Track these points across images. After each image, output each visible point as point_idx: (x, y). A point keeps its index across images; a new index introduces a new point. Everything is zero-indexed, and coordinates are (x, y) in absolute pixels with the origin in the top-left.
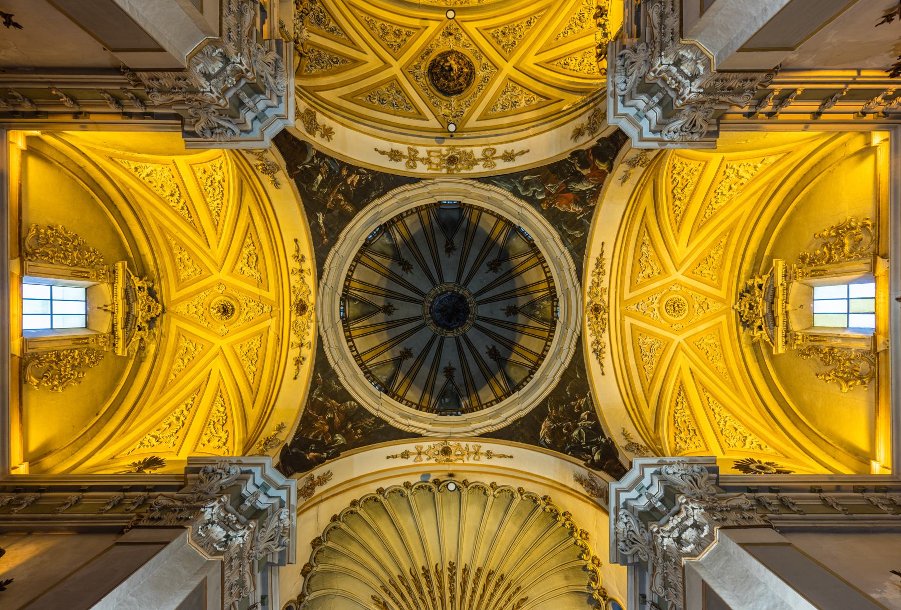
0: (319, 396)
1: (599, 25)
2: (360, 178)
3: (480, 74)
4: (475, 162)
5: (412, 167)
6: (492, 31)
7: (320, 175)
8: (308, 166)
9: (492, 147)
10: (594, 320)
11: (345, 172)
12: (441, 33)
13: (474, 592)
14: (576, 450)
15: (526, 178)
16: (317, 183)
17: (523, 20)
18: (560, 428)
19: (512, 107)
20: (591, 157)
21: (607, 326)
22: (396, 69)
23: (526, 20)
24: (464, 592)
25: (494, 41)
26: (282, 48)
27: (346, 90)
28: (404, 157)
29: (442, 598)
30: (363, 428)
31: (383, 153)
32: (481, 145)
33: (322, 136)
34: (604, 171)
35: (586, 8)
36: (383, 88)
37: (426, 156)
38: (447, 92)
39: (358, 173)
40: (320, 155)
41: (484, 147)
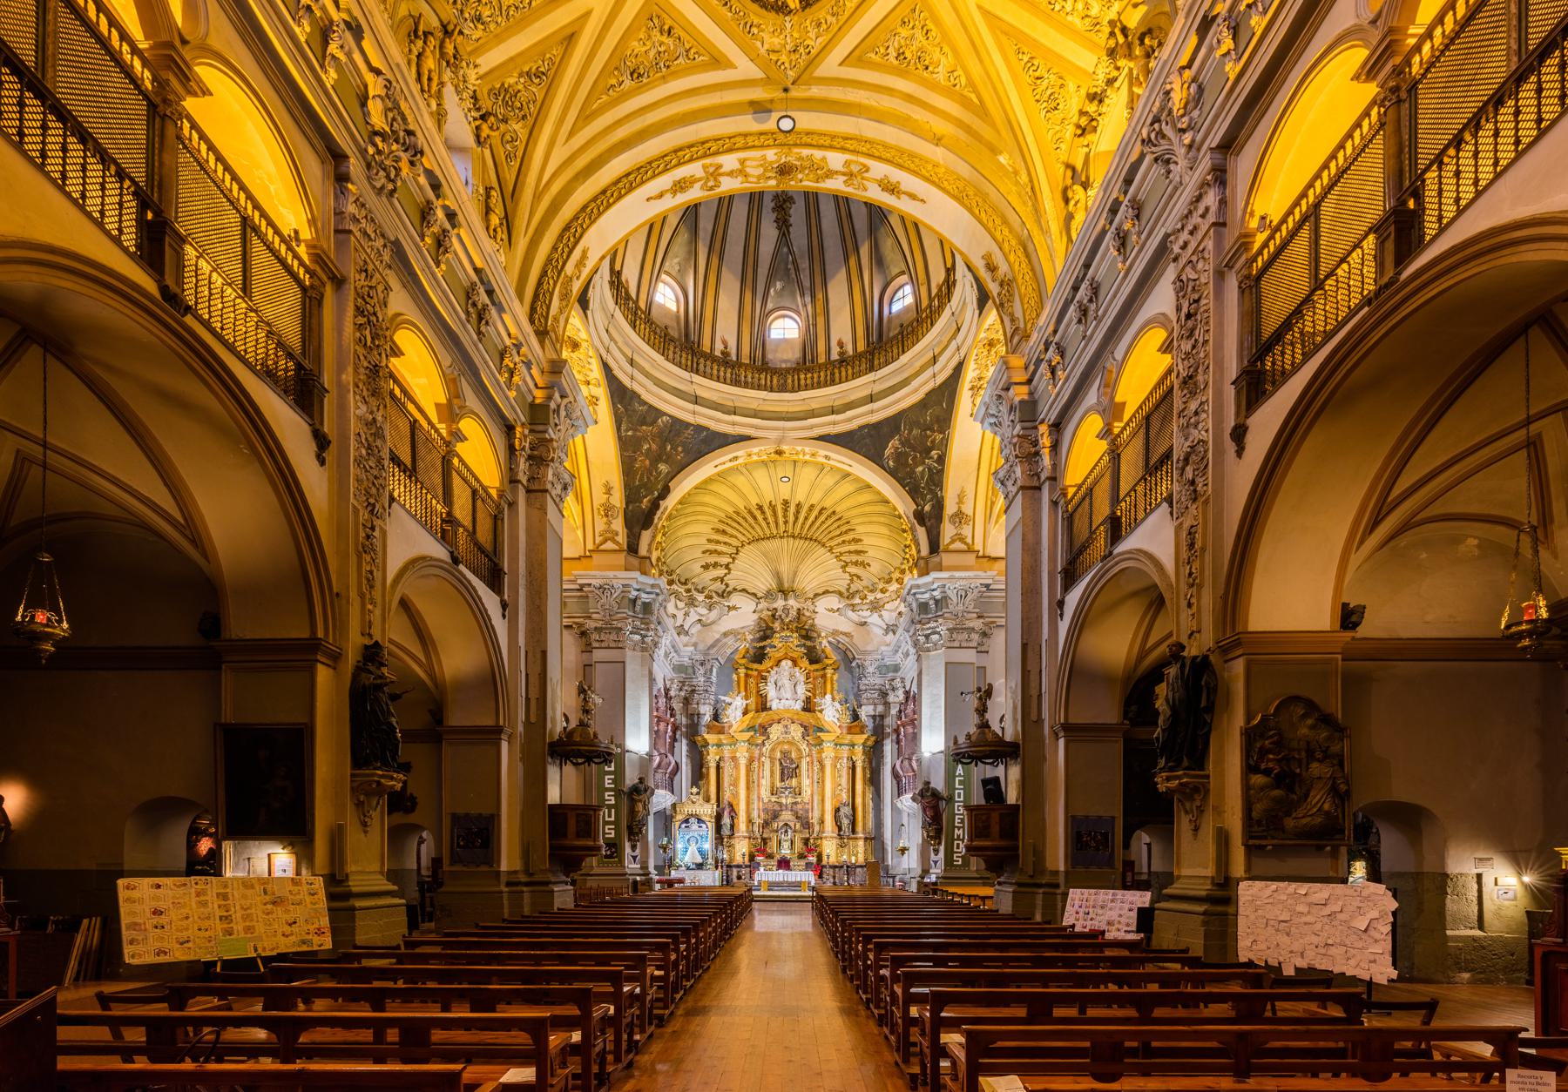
0: (627, 430)
4: (830, 174)
5: (711, 189)
13: (806, 518)
14: (914, 492)
18: (906, 455)
24: (796, 518)
29: (777, 523)
30: (683, 444)
37: (737, 166)
41: (848, 156)
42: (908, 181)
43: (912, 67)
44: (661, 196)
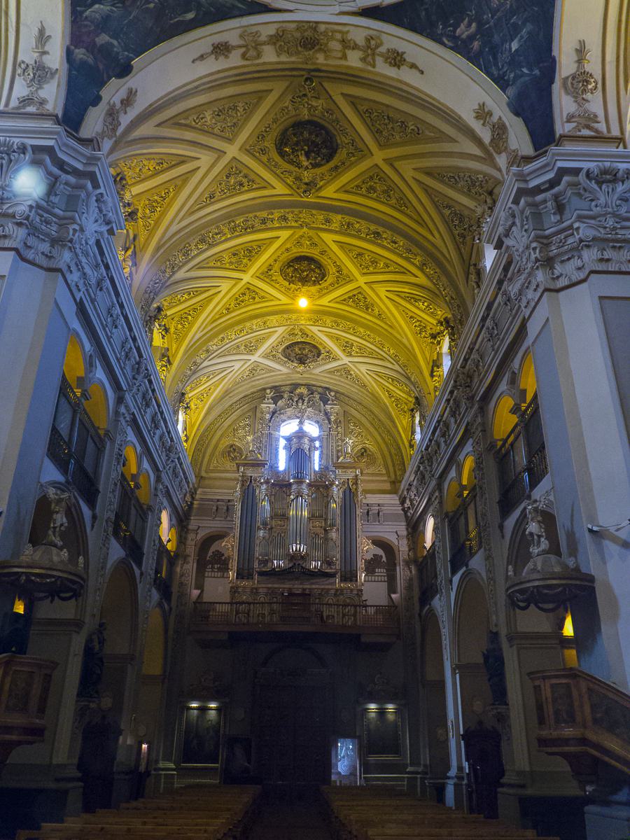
1: (129, 205)
2: (454, 31)
3: (269, 144)
6: (255, 186)
7: (513, 50)
8: (525, 70)
11: (476, 45)
15: (190, 16)
16: (522, 37)
17: (220, 198)
19: (224, 109)
20: (101, 67)
22: (379, 156)
23: (215, 199)
25: (252, 176)
27: (448, 147)
28: (381, 55)
31: (413, 66)
32: (264, 63)
33: (490, 114)
34: (76, 47)
35: (149, 218)
37: (350, 53)
38: (314, 125)
39: (454, 38)
40: (502, 83)
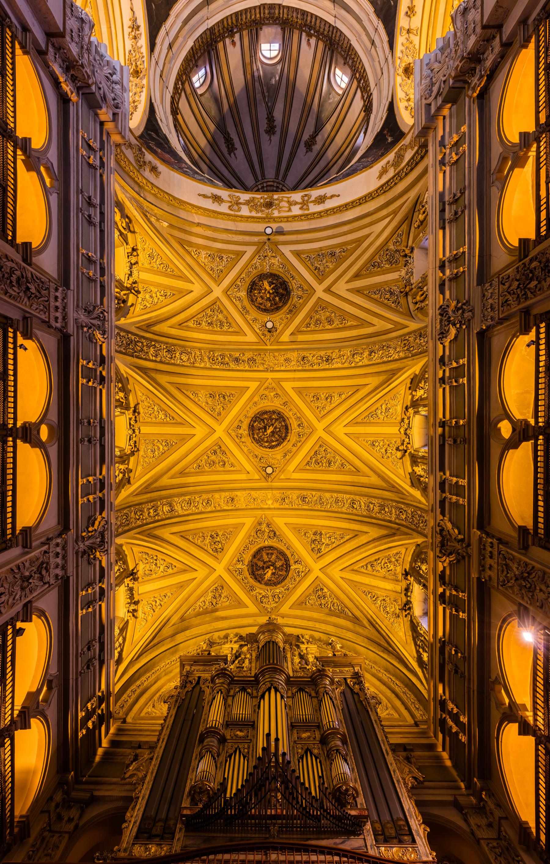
4: (247, 203)
5: (306, 195)
9: (232, 213)
10: (138, 63)
12: (278, 331)
21: (127, 58)
26: (425, 114)
36: (331, 266)
37: (293, 208)
42: (208, 204)
43: (216, 254)
44: (332, 196)
